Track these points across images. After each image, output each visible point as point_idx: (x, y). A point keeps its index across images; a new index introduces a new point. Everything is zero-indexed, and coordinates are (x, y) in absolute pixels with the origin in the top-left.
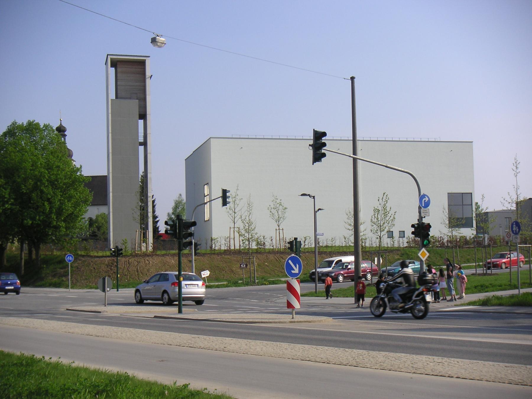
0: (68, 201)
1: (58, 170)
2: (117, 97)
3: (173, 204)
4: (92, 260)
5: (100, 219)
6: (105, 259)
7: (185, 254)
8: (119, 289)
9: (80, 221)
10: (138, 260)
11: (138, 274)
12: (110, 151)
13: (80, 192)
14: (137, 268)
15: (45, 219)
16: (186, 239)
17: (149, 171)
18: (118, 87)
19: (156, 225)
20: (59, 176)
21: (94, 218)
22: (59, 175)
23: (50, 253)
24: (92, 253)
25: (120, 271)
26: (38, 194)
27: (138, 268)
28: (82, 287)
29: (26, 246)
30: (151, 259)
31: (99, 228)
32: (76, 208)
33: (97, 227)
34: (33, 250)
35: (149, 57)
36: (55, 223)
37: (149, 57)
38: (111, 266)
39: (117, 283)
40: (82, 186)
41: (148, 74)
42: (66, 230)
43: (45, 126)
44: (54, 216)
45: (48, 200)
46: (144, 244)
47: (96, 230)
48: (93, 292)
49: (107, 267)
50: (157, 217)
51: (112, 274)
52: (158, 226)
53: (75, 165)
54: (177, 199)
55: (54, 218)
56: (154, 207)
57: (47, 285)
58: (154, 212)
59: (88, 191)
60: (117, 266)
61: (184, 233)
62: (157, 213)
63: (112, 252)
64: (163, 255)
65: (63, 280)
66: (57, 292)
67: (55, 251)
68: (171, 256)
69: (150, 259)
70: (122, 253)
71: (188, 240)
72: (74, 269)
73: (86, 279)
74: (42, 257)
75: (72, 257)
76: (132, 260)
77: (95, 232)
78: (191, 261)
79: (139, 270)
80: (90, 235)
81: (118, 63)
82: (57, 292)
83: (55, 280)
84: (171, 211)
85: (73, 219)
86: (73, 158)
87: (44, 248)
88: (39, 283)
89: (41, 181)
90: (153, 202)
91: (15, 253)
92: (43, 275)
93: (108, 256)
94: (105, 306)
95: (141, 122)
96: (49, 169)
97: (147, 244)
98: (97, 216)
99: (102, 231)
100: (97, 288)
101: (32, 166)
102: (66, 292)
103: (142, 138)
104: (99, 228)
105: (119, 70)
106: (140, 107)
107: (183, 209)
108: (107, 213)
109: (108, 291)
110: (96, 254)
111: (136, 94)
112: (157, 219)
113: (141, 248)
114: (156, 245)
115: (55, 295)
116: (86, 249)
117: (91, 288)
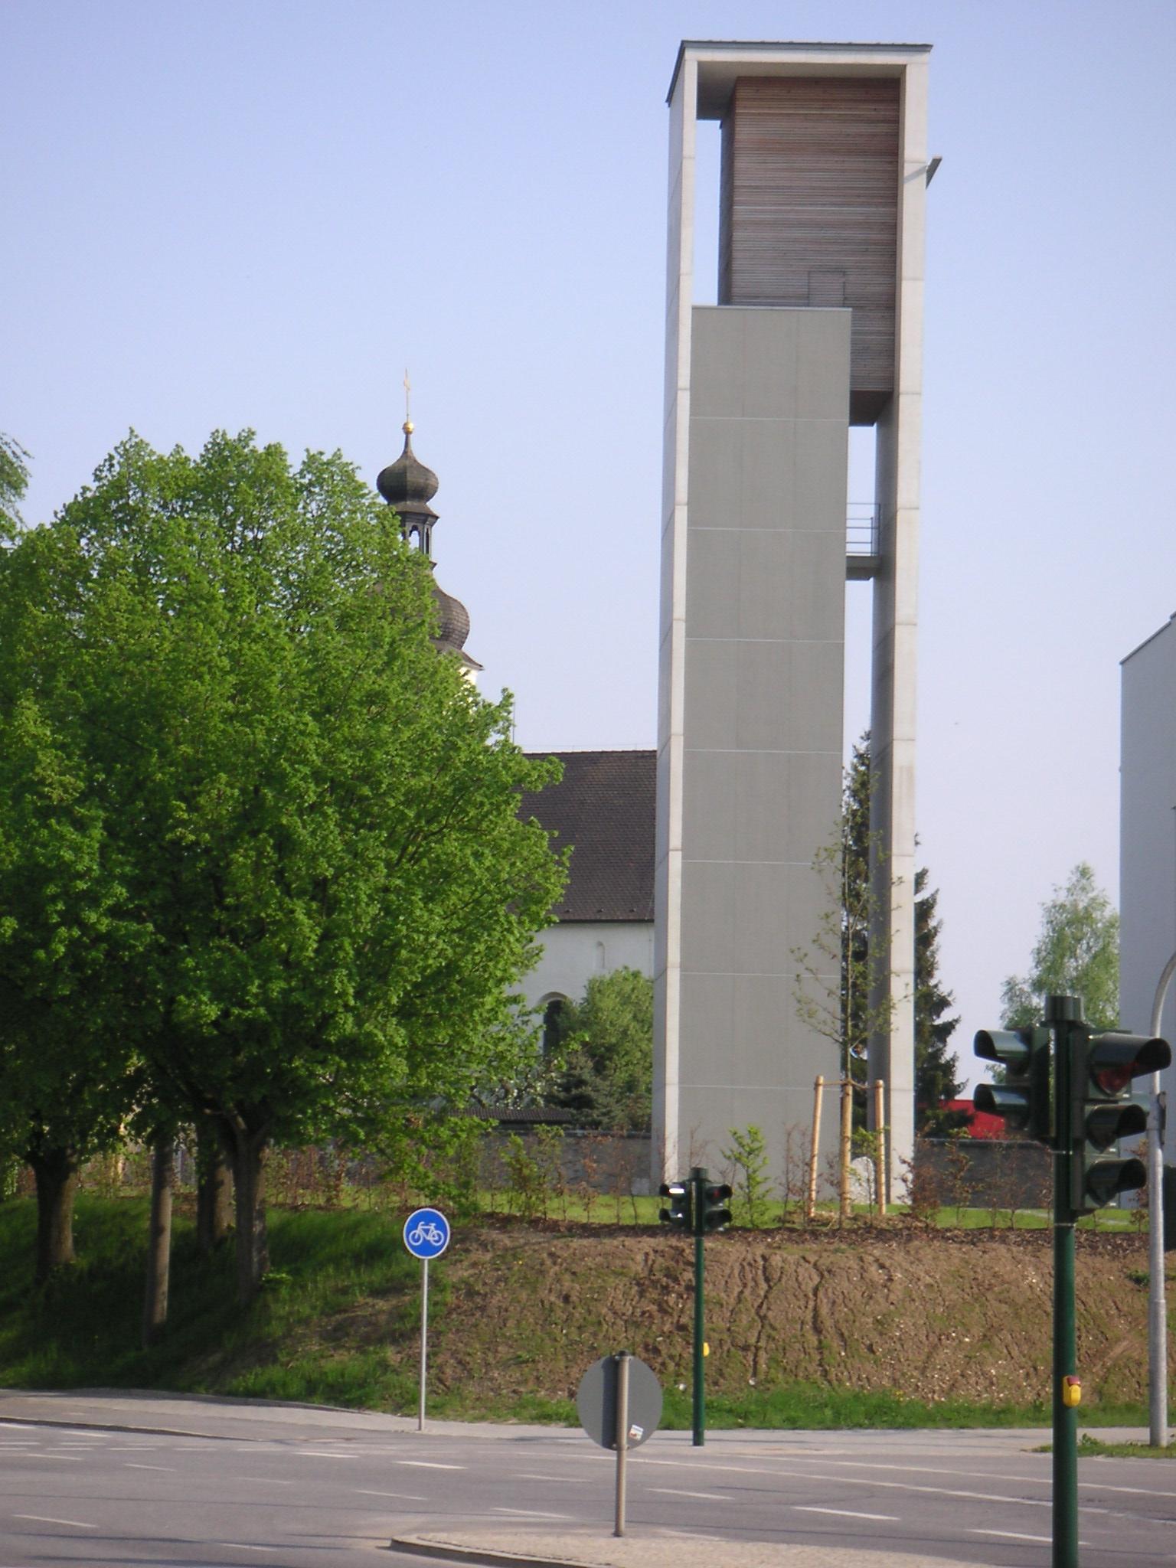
0: (428, 899)
1: (377, 720)
2: (726, 295)
3: (1035, 932)
4: (557, 1245)
5: (608, 1003)
6: (630, 1242)
7: (1109, 1236)
8: (708, 1434)
9: (493, 1010)
10: (825, 1261)
11: (820, 1348)
12: (680, 610)
13: (495, 847)
14: (815, 1309)
15: (297, 997)
16: (1102, 1144)
17: (900, 728)
18: (738, 235)
19: (938, 1053)
20: (379, 756)
21: (576, 995)
22: (381, 744)
23: (322, 1201)
24: (553, 1204)
25: (715, 1321)
26: (260, 854)
27: (824, 1311)
28: (489, 1410)
29: (184, 1160)
30: (900, 1256)
31: (601, 1057)
32: (473, 938)
33: (589, 1049)
34: (226, 1175)
35: (925, 48)
36: (347, 1024)
37: (925, 48)
38: (666, 1289)
39: (697, 1395)
40: (511, 810)
41: (915, 151)
42: (414, 1068)
43: (311, 462)
44: (343, 983)
45: (319, 888)
46: (861, 1167)
47: (585, 1067)
48: (554, 1441)
49: (642, 1294)
50: (943, 1003)
51: (669, 1336)
52: (947, 1056)
53: (472, 691)
54: (1062, 897)
55: (343, 994)
56: (924, 939)
57: (295, 1387)
58: (924, 969)
59: (540, 839)
60: (696, 1289)
61: (1089, 1108)
62: (944, 980)
63: (668, 1205)
64: (974, 1237)
65: (384, 1366)
66: (349, 1437)
67: (346, 1186)
68: (1023, 1242)
69: (896, 1255)
70: (726, 1216)
71: (1123, 1149)
72: (450, 1298)
73: (519, 1362)
74: (273, 1218)
75: (440, 1226)
76: (786, 1256)
77: (581, 1083)
78: (1142, 1282)
79: (828, 1323)
80: (549, 1098)
81: (742, 93)
82: (349, 1437)
83: (342, 1361)
84: (1026, 970)
85: (452, 1001)
86: (466, 648)
87: (287, 1166)
88: (251, 1378)
89: (274, 778)
90: (924, 911)
91: (127, 1192)
92: (276, 1329)
93: (649, 1230)
94: (617, 1534)
95: (863, 439)
96: (328, 709)
97: (876, 1164)
98: (596, 989)
99: (621, 1077)
100: (573, 1421)
101: (241, 689)
102: (400, 1436)
103: (867, 535)
104: (601, 1057)
105: (745, 131)
106: (859, 351)
107: (1101, 958)
108: (648, 972)
109: (633, 1443)
110: (577, 1214)
111: (842, 272)
112: (946, 1016)
113: (839, 1184)
114: (929, 1171)
115: (338, 1453)
116: (522, 1183)
117: (545, 1418)
